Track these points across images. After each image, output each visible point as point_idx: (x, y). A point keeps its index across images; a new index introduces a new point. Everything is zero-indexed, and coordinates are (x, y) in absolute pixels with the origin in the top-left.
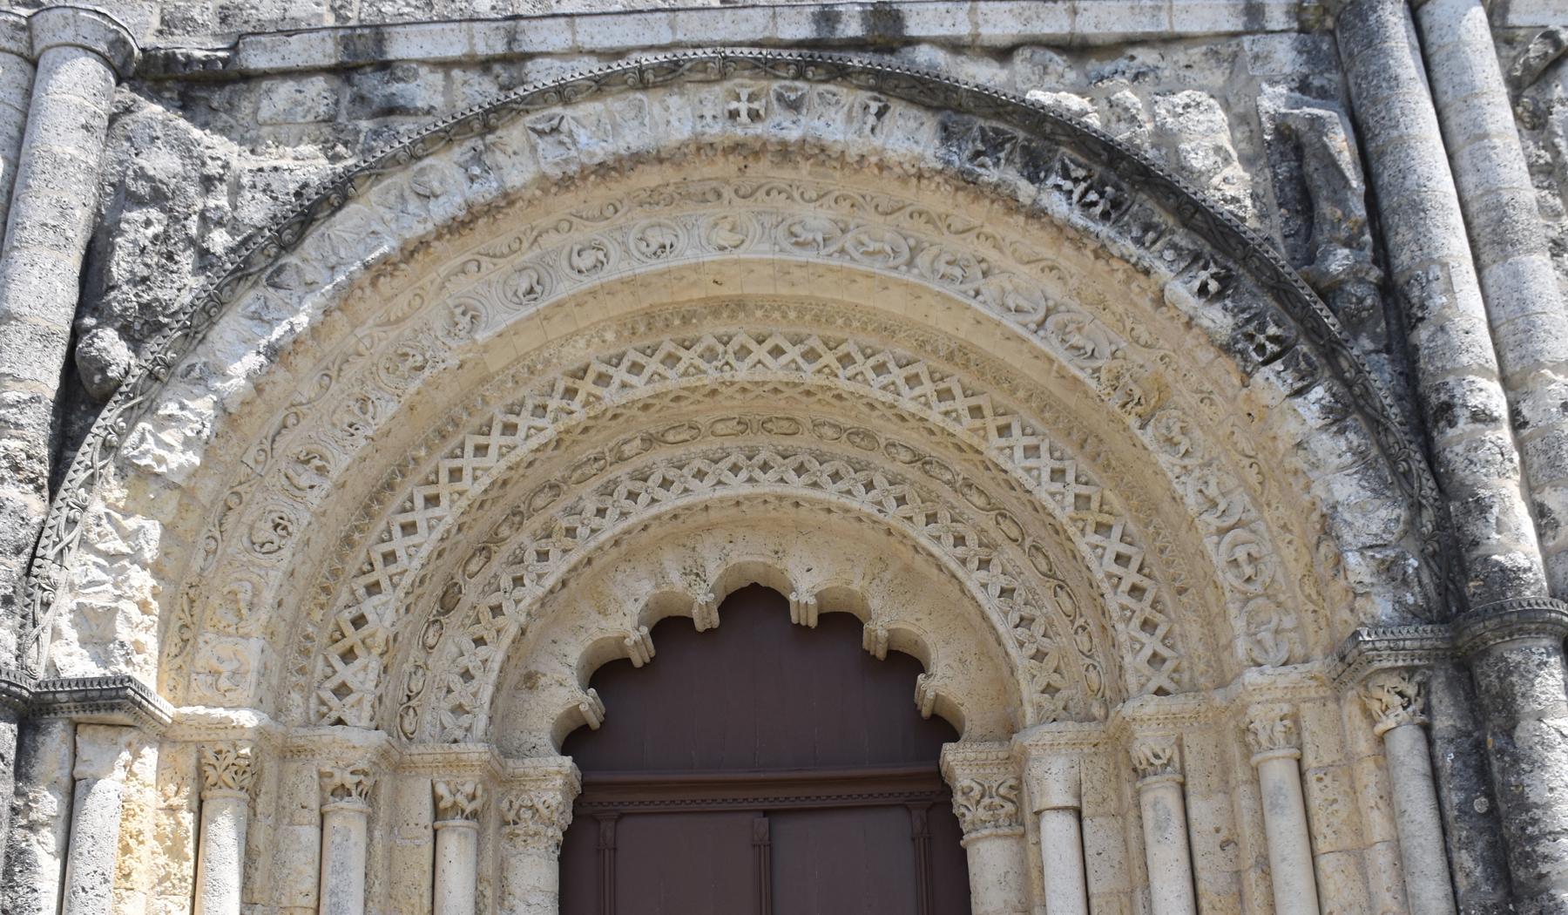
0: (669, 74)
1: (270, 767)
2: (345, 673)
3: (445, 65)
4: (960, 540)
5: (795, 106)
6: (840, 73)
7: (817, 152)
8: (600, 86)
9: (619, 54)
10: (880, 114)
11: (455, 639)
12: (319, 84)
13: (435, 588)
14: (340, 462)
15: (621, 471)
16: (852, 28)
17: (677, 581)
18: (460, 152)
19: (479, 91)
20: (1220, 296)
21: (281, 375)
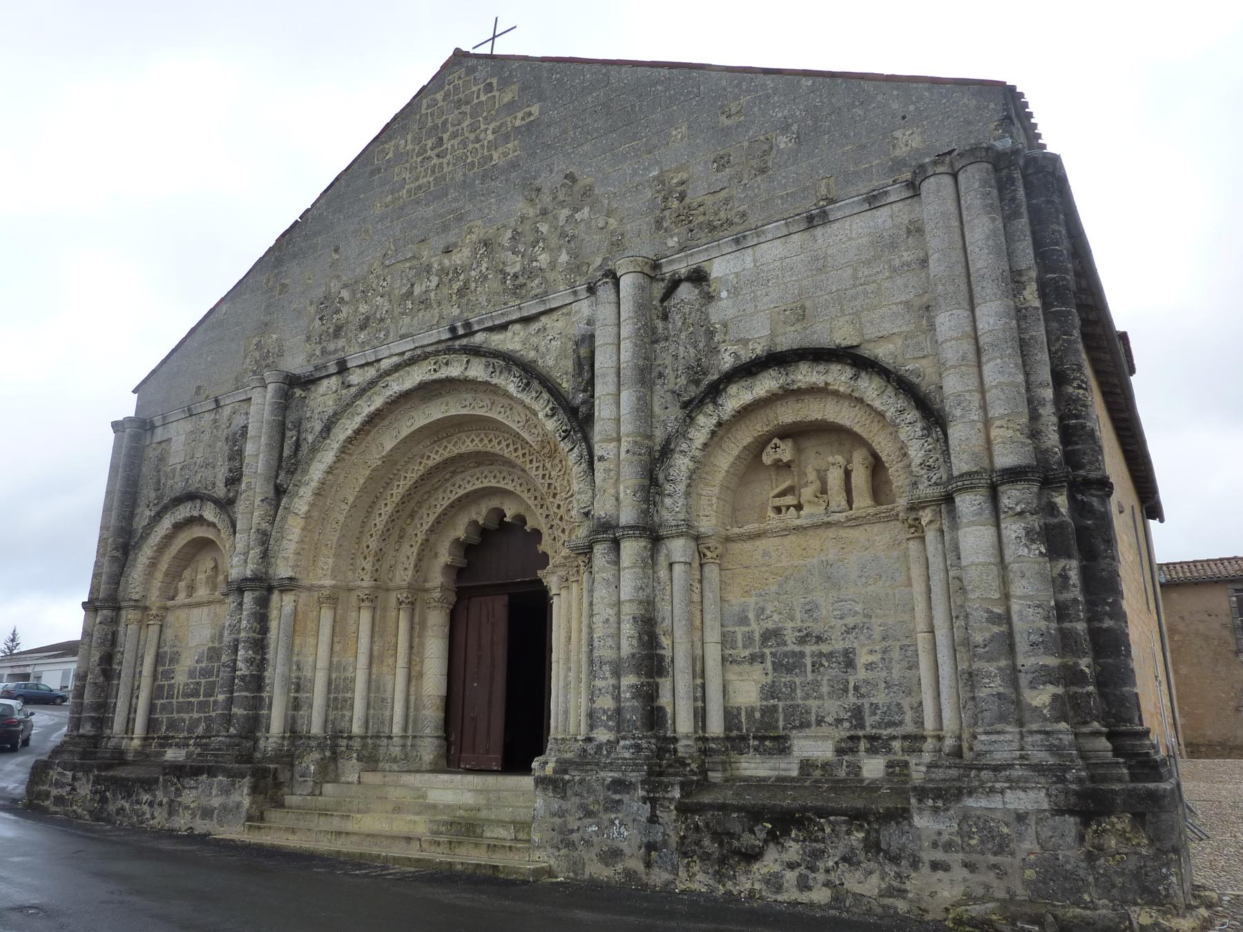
0: (412, 361)
1: (342, 595)
2: (364, 564)
3: (362, 366)
4: (536, 498)
5: (447, 364)
6: (455, 351)
7: (450, 382)
8: (397, 368)
9: (403, 353)
10: (468, 362)
11: (406, 546)
12: (334, 379)
13: (396, 533)
14: (351, 499)
15: (448, 484)
16: (461, 332)
17: (474, 517)
18: (365, 398)
19: (371, 373)
20: (552, 416)
21: (330, 477)
